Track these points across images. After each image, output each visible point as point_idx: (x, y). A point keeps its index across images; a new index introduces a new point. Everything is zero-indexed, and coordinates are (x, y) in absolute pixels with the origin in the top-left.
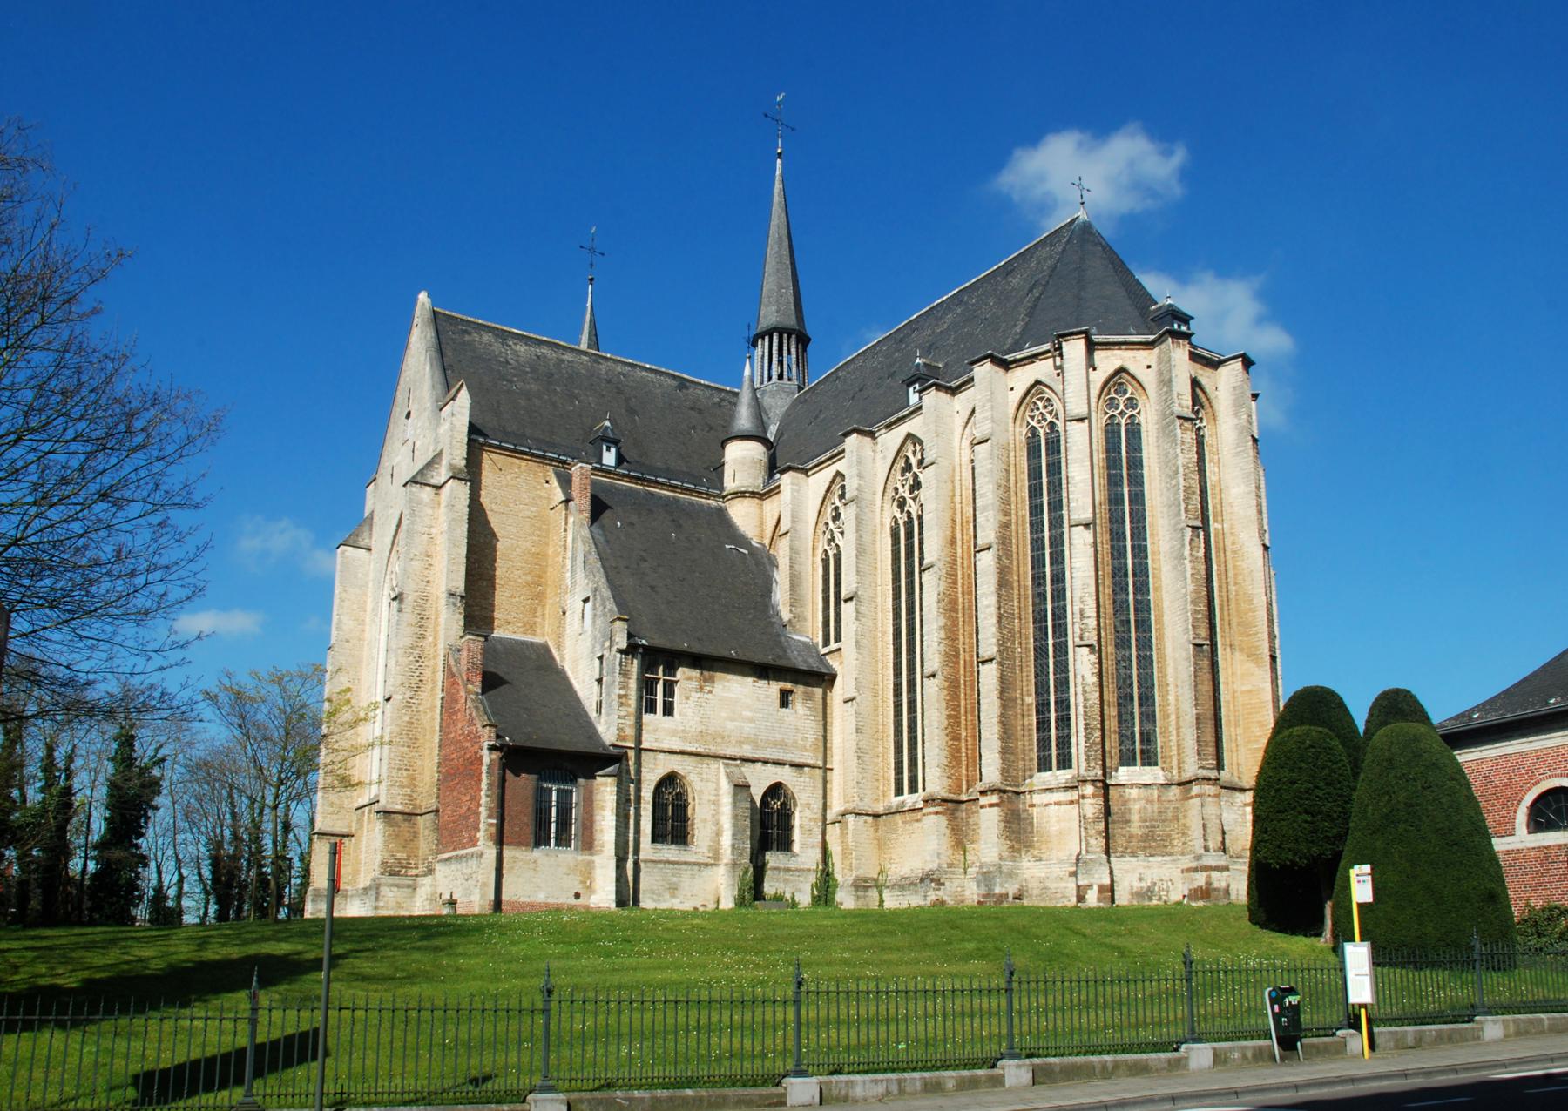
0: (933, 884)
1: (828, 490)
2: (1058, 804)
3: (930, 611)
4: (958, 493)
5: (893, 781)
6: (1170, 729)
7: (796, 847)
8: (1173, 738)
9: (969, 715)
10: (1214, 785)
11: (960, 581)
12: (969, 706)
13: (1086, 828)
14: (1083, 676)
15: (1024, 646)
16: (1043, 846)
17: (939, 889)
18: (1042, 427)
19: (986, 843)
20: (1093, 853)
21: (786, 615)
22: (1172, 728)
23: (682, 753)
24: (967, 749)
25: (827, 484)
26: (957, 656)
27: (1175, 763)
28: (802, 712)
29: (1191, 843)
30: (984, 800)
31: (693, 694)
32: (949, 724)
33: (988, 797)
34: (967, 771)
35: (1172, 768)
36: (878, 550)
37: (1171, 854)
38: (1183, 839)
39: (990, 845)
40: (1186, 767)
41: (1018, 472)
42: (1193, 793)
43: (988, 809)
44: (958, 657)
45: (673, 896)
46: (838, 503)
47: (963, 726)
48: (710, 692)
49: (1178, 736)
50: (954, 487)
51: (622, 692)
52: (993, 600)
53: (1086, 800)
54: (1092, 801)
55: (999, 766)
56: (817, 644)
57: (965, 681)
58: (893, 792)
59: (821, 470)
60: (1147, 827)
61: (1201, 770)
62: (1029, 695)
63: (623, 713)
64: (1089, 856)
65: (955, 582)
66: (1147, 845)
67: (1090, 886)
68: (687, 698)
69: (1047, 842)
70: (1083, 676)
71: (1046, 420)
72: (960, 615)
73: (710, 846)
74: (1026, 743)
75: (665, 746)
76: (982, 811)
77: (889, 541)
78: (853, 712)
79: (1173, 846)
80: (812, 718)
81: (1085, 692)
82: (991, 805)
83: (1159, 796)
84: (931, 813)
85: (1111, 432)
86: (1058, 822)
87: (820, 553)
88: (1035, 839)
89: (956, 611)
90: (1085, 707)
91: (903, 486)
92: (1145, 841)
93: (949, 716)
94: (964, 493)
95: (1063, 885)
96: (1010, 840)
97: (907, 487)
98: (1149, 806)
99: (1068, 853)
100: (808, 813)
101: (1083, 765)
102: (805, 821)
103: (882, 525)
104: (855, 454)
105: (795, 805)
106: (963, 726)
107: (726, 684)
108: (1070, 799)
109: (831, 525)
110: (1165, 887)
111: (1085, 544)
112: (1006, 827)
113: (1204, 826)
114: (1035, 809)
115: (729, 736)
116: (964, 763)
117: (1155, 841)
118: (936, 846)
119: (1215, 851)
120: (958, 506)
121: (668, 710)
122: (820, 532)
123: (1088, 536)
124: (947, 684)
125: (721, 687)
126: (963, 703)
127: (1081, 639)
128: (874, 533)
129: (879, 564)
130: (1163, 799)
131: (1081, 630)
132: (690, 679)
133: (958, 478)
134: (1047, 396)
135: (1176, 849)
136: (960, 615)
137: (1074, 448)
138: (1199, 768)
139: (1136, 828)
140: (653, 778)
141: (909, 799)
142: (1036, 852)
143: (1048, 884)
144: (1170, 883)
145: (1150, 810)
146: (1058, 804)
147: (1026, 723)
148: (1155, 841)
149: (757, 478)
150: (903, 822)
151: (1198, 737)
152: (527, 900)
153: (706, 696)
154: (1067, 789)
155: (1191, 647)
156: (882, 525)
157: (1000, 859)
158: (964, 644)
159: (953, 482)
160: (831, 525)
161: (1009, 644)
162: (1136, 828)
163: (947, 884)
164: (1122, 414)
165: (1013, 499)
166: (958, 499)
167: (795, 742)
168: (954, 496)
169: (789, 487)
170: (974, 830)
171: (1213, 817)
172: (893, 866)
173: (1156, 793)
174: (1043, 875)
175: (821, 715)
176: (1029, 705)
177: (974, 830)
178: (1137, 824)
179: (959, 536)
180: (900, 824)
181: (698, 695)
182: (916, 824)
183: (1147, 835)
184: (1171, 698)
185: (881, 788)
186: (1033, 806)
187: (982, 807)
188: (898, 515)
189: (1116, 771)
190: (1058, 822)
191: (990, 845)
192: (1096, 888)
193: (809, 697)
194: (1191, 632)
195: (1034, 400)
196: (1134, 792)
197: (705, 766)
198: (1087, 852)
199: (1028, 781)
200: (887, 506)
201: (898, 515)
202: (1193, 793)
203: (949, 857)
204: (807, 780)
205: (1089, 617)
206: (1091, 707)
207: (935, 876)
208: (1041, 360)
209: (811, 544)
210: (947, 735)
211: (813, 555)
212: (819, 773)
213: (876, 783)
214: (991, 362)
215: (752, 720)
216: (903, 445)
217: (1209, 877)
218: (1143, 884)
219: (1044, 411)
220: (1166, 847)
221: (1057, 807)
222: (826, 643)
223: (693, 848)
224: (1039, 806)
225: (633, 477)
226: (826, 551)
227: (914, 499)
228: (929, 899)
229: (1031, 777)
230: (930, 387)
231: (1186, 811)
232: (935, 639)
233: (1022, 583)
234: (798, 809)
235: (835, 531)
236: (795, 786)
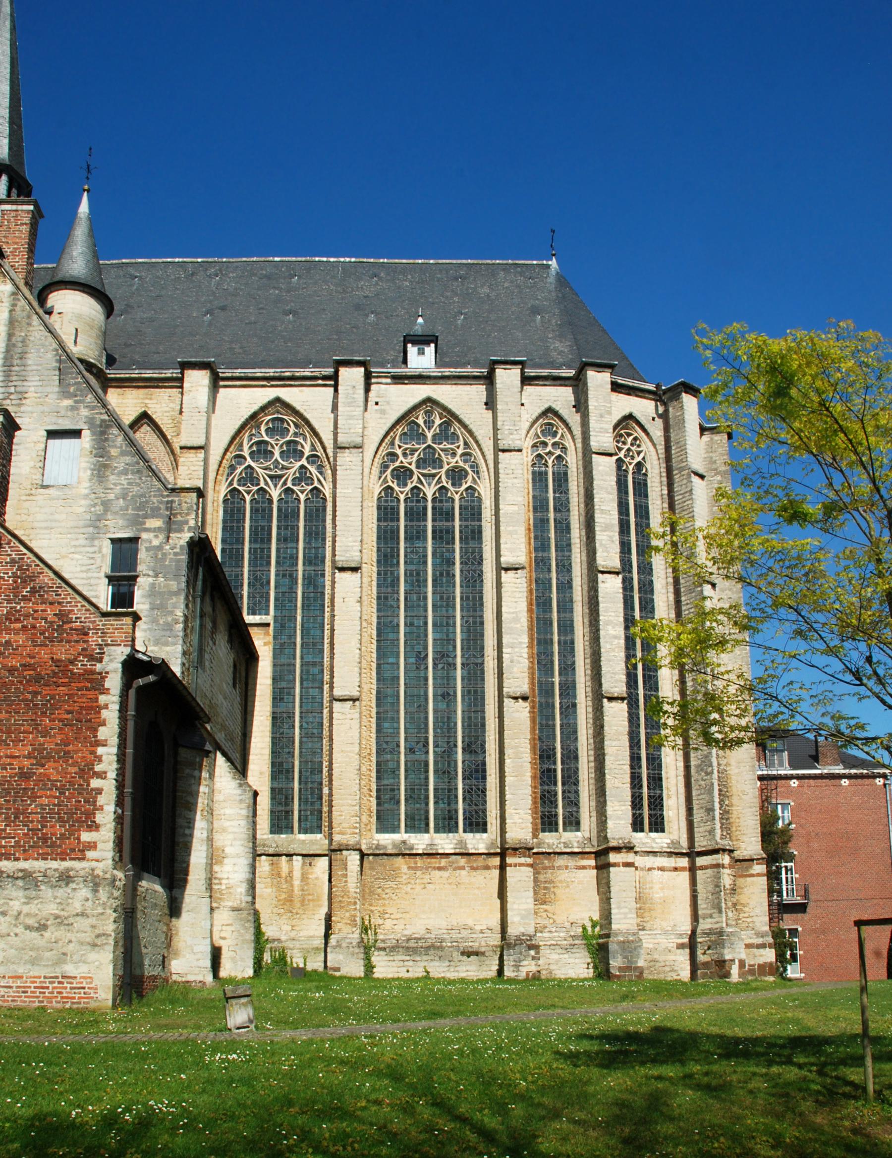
16: (646, 914)
20: (731, 926)
25: (256, 408)
39: (627, 910)
43: (622, 868)
69: (650, 910)
84: (521, 865)
86: (662, 889)
99: (672, 924)
143: (656, 956)
170: (545, 888)
177: (545, 888)
182: (437, 873)
187: (615, 865)
190: (662, 889)
191: (627, 910)
198: (727, 925)
216: (415, 408)
221: (660, 872)
224: (642, 869)
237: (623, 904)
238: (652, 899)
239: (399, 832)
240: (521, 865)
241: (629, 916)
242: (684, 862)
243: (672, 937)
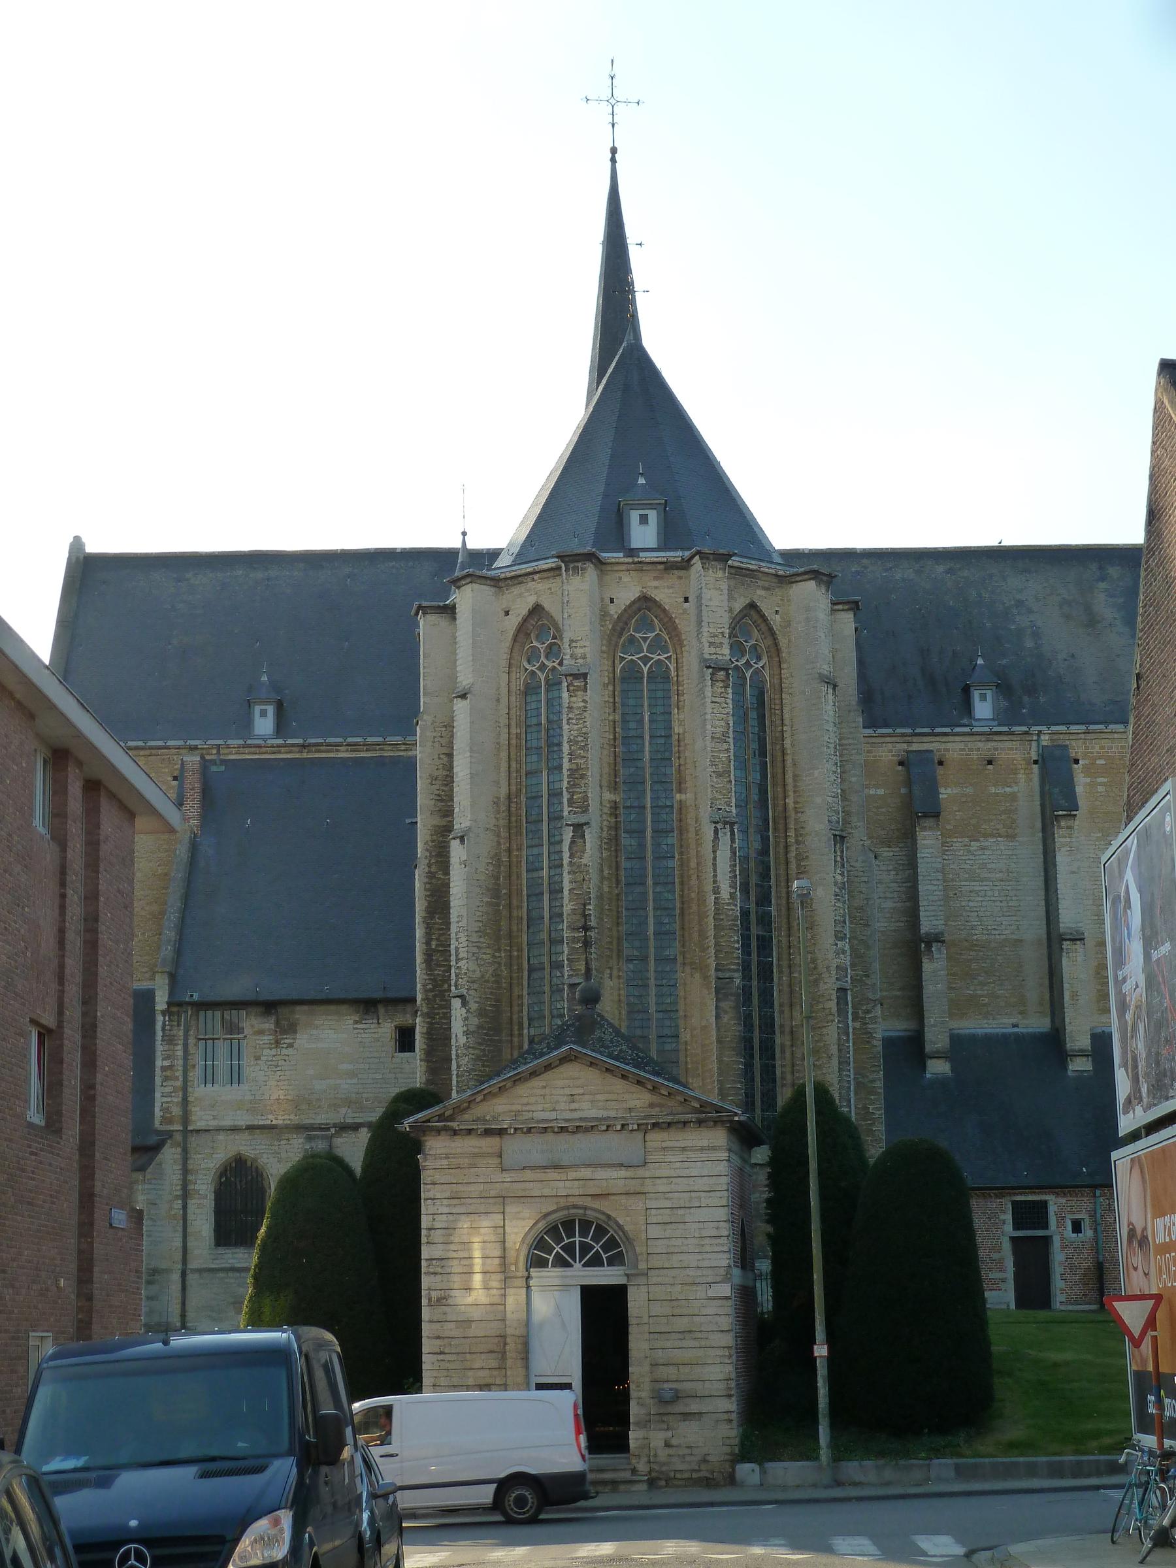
23: (251, 1128)
31: (266, 1052)
48: (290, 1046)
51: (166, 1063)
63: (167, 1090)
68: (257, 1058)
75: (227, 1123)
107: (314, 1032)
115: (319, 1100)
121: (236, 1076)
125: (305, 1036)
132: (261, 1032)
140: (212, 1165)
153: (284, 1051)
181: (273, 1052)
197: (283, 1142)
215: (352, 1074)
225: (293, 745)
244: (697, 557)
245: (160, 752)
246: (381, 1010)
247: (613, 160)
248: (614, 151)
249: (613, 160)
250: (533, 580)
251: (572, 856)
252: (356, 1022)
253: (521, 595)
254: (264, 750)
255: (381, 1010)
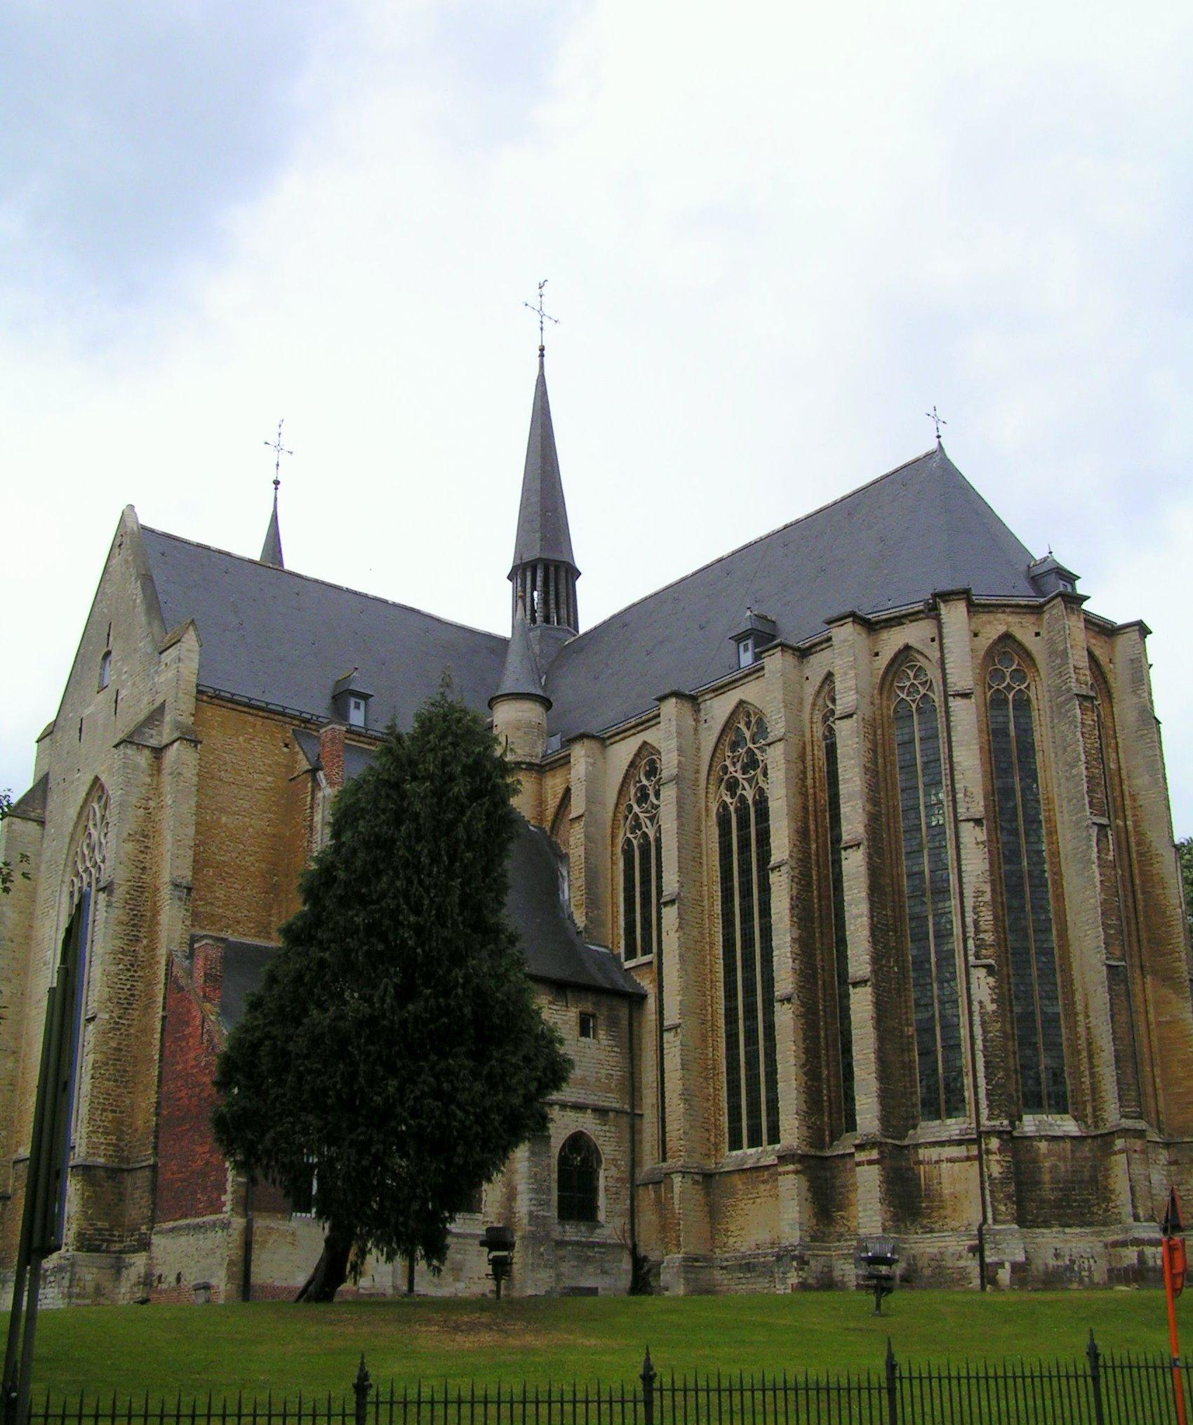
0: (795, 1263)
1: (632, 764)
2: (950, 1160)
3: (781, 919)
4: (810, 774)
5: (726, 1130)
6: (1082, 1068)
7: (601, 1216)
8: (1086, 1080)
9: (831, 1049)
10: (1139, 1138)
11: (815, 883)
12: (830, 1038)
13: (992, 1192)
14: (981, 1002)
15: (901, 963)
17: (802, 1269)
18: (914, 701)
19: (865, 1210)
20: (1004, 1222)
21: (580, 920)
22: (1084, 1067)
24: (829, 1091)
26: (814, 975)
27: (1089, 1110)
28: (605, 1042)
29: (1116, 1211)
30: (861, 1156)
32: (807, 1060)
33: (867, 1153)
34: (830, 1118)
35: (1086, 1116)
36: (704, 841)
37: (1090, 1224)
38: (1104, 1206)
40: (1105, 1115)
41: (887, 754)
42: (1116, 1148)
43: (866, 1167)
44: (815, 978)
45: (457, 1280)
46: (645, 782)
47: (823, 1063)
49: (1092, 1075)
50: (805, 768)
52: (864, 908)
53: (991, 1157)
54: (998, 1157)
55: (878, 1114)
56: (619, 954)
57: (825, 1006)
58: (727, 1146)
59: (623, 739)
60: (1061, 1190)
61: (1123, 1120)
62: (908, 1025)
64: (997, 1227)
65: (809, 884)
66: (1061, 1211)
67: (1001, 1265)
70: (981, 1002)
71: (918, 692)
72: (816, 925)
73: (499, 1214)
74: (908, 1085)
76: (858, 1169)
77: (715, 832)
78: (678, 1043)
79: (1093, 1213)
80: (618, 1050)
81: (983, 1023)
82: (870, 1162)
83: (1073, 1151)
84: (788, 1173)
85: (997, 702)
87: (620, 841)
88: (924, 1205)
89: (812, 920)
90: (984, 1040)
91: (734, 764)
92: (1059, 1208)
93: (807, 1051)
94: (817, 775)
95: (962, 1263)
96: (894, 1207)
97: (739, 766)
98: (1061, 1164)
99: (966, 1222)
100: (613, 1172)
101: (984, 1112)
102: (611, 1183)
103: (707, 810)
104: (674, 723)
105: (599, 1162)
106: (823, 1063)
108: (965, 1154)
109: (636, 809)
110: (1086, 1266)
111: (977, 843)
112: (888, 1190)
113: (1132, 1189)
114: (922, 1167)
116: (826, 1109)
117: (1071, 1207)
118: (797, 1215)
119: (1146, 1221)
120: (811, 791)
122: (621, 817)
123: (981, 834)
124: (803, 1010)
126: (822, 1034)
127: (977, 957)
128: (699, 819)
129: (705, 858)
130: (1078, 1154)
131: (976, 946)
133: (809, 758)
134: (919, 664)
135: (1096, 1218)
136: (816, 925)
137: (959, 728)
138: (1122, 1117)
139: (1048, 1193)
141: (749, 1155)
142: (925, 1222)
144: (1091, 1261)
145: (1063, 1170)
146: (950, 1160)
147: (907, 1060)
148: (1071, 1207)
149: (533, 746)
150: (744, 1183)
151: (1118, 1079)
152: (285, 1284)
154: (959, 1143)
155: (1104, 968)
156: (707, 810)
157: (884, 1230)
158: (822, 960)
159: (803, 762)
160: (636, 809)
161: (884, 962)
162: (1048, 1193)
163: (812, 1263)
164: (1009, 688)
165: (882, 785)
166: (809, 782)
167: (598, 1080)
168: (804, 780)
169: (583, 760)
171: (1142, 1177)
172: (731, 1240)
173: (1068, 1146)
174: (936, 1251)
175: (627, 1045)
176: (909, 1037)
178: (1047, 1186)
179: (812, 827)
180: (741, 1187)
182: (762, 1187)
183: (1061, 1200)
184: (1081, 1030)
185: (712, 1139)
186: (921, 1163)
187: (859, 1164)
188: (729, 800)
189: (1020, 1119)
192: (1007, 1265)
193: (613, 1023)
194: (1104, 951)
195: (903, 668)
196: (1043, 1146)
198: (995, 1221)
199: (911, 1132)
200: (712, 788)
201: (729, 800)
202: (1116, 1148)
203: (812, 1228)
204: (613, 1129)
205: (985, 931)
206: (992, 1041)
207: (796, 1253)
208: (911, 621)
209: (609, 831)
210: (805, 1074)
211: (613, 845)
212: (625, 1121)
213: (707, 1135)
214: (854, 622)
217: (1141, 1256)
218: (1060, 1263)
219: (915, 682)
220: (1083, 1214)
221: (949, 1164)
222: (631, 954)
223: (479, 1216)
226: (629, 841)
227: (749, 781)
228: (790, 1282)
229: (915, 1127)
230: (776, 647)
231: (1107, 1170)
232: (789, 955)
233: (896, 888)
234: (603, 1166)
235: (641, 815)
236: (598, 1137)
237: (869, 1206)
238: (940, 1196)
239: (741, 1148)
240: (788, 1173)
241: (874, 1219)
242: (974, 1151)
243: (964, 1238)
244: (1137, 628)
245: (276, 717)
246: (570, 995)
247: (542, 356)
248: (542, 349)
249: (542, 356)
250: (1004, 612)
251: (1099, 852)
252: (550, 1003)
253: (990, 622)
254: (362, 739)
255: (570, 995)
